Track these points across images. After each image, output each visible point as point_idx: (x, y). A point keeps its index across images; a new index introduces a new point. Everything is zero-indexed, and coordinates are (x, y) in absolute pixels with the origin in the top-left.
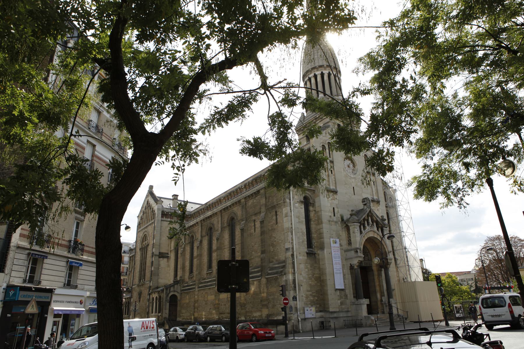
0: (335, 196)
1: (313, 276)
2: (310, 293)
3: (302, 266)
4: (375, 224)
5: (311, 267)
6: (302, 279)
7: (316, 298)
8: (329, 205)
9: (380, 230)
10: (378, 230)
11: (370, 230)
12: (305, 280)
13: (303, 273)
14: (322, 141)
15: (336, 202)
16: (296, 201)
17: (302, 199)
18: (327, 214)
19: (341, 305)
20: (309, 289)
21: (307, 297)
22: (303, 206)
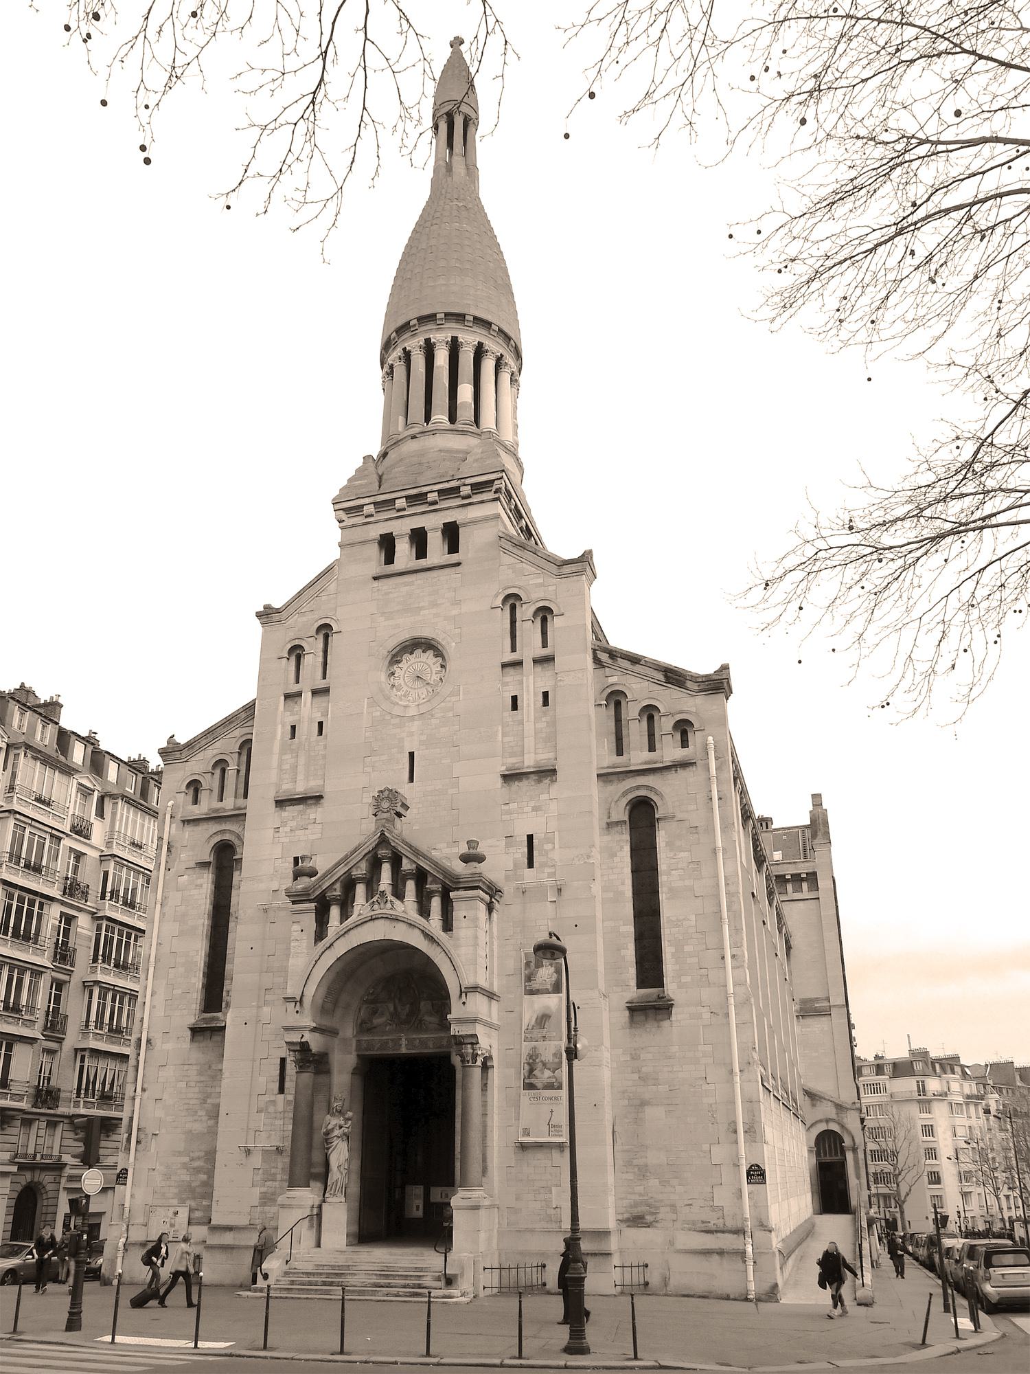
0: (314, 813)
1: (204, 1101)
2: (186, 1159)
3: (169, 1073)
4: (410, 886)
5: (200, 1073)
6: (160, 1113)
7: (203, 1177)
8: (278, 851)
9: (436, 903)
10: (424, 911)
11: (367, 913)
12: (169, 1119)
13: (166, 1097)
14: (291, 635)
15: (313, 833)
16: (184, 866)
17: (207, 856)
18: (262, 886)
19: (263, 1204)
20: (181, 1146)
21: (167, 1177)
22: (206, 881)
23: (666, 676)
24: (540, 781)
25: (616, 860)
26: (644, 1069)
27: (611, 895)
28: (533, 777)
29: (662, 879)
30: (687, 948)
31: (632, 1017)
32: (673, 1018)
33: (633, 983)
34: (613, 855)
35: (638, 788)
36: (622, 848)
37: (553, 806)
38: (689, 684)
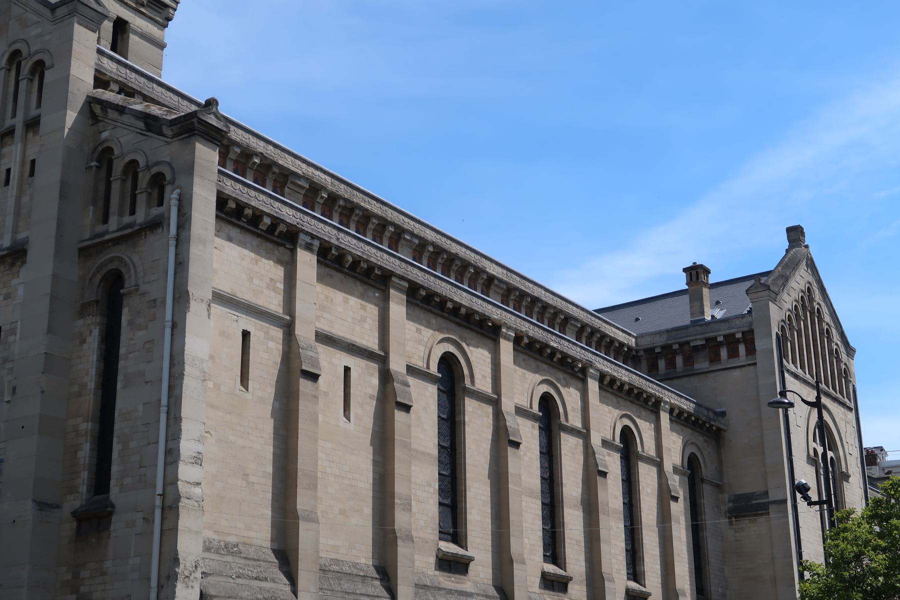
23: (146, 124)
24: (13, 264)
25: (85, 346)
26: (83, 589)
27: (76, 388)
28: (9, 260)
29: (121, 364)
30: (133, 444)
31: (79, 528)
32: (112, 528)
33: (83, 489)
34: (83, 341)
35: (111, 260)
36: (91, 332)
37: (21, 291)
38: (166, 130)
